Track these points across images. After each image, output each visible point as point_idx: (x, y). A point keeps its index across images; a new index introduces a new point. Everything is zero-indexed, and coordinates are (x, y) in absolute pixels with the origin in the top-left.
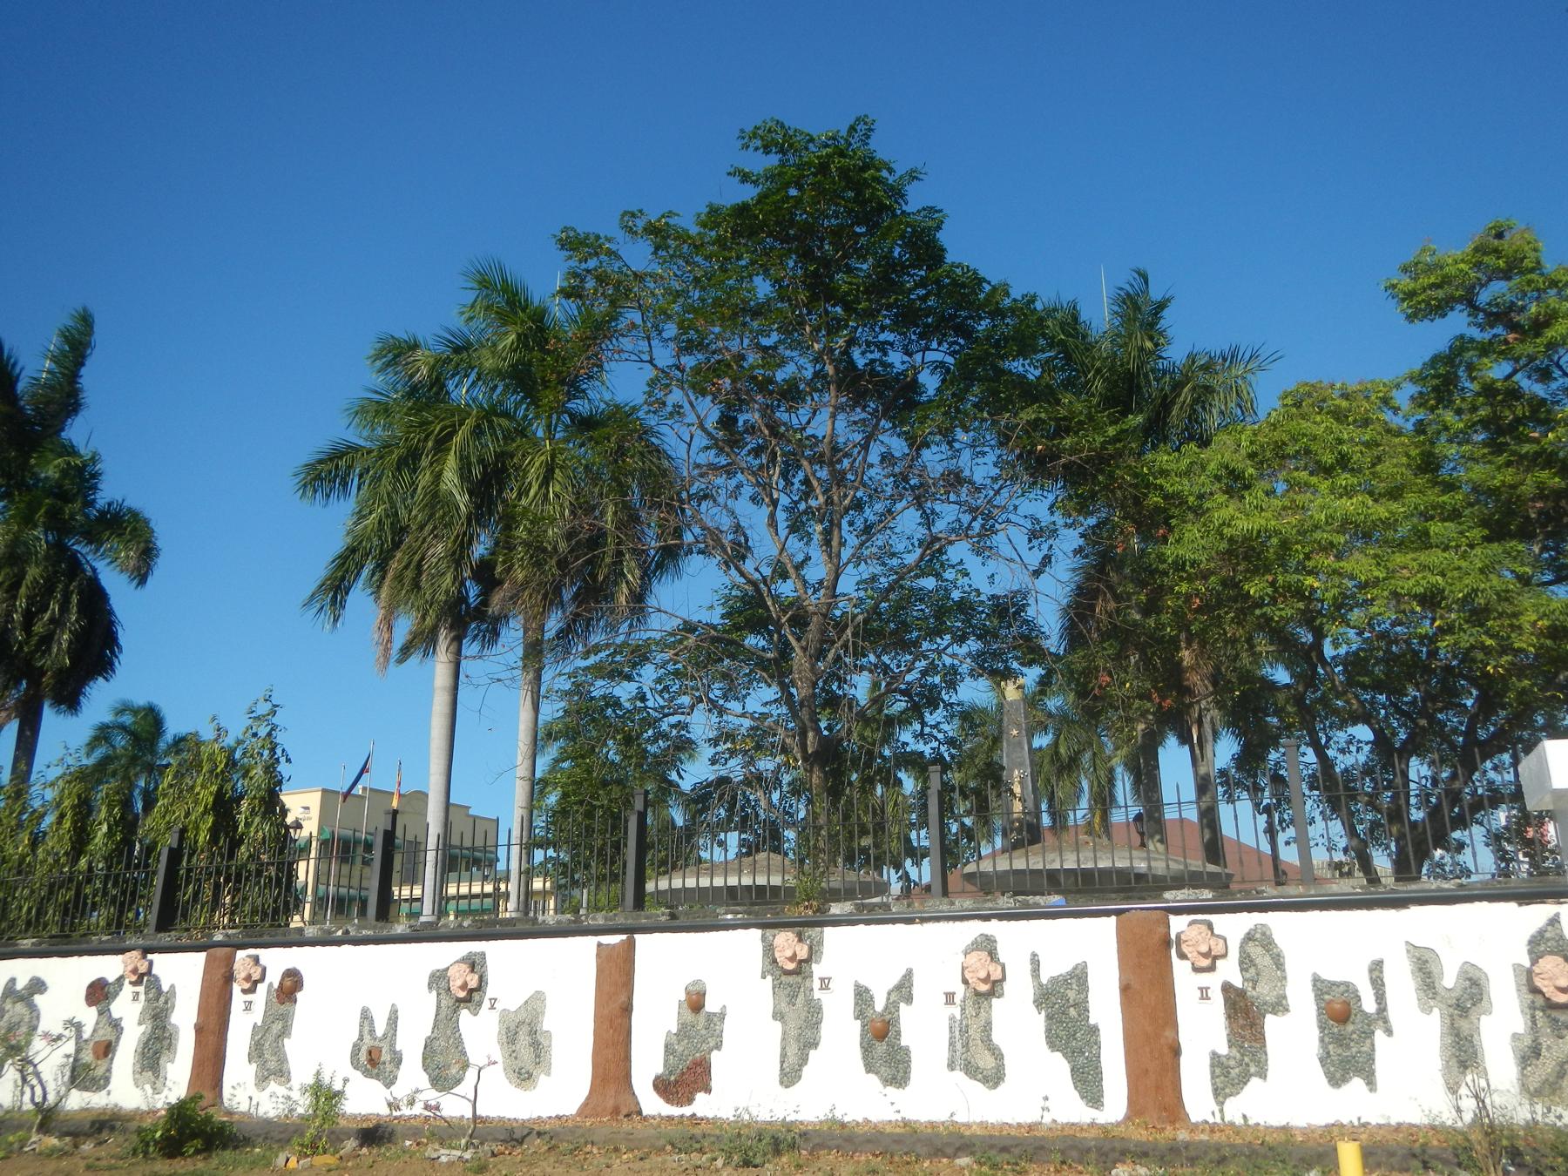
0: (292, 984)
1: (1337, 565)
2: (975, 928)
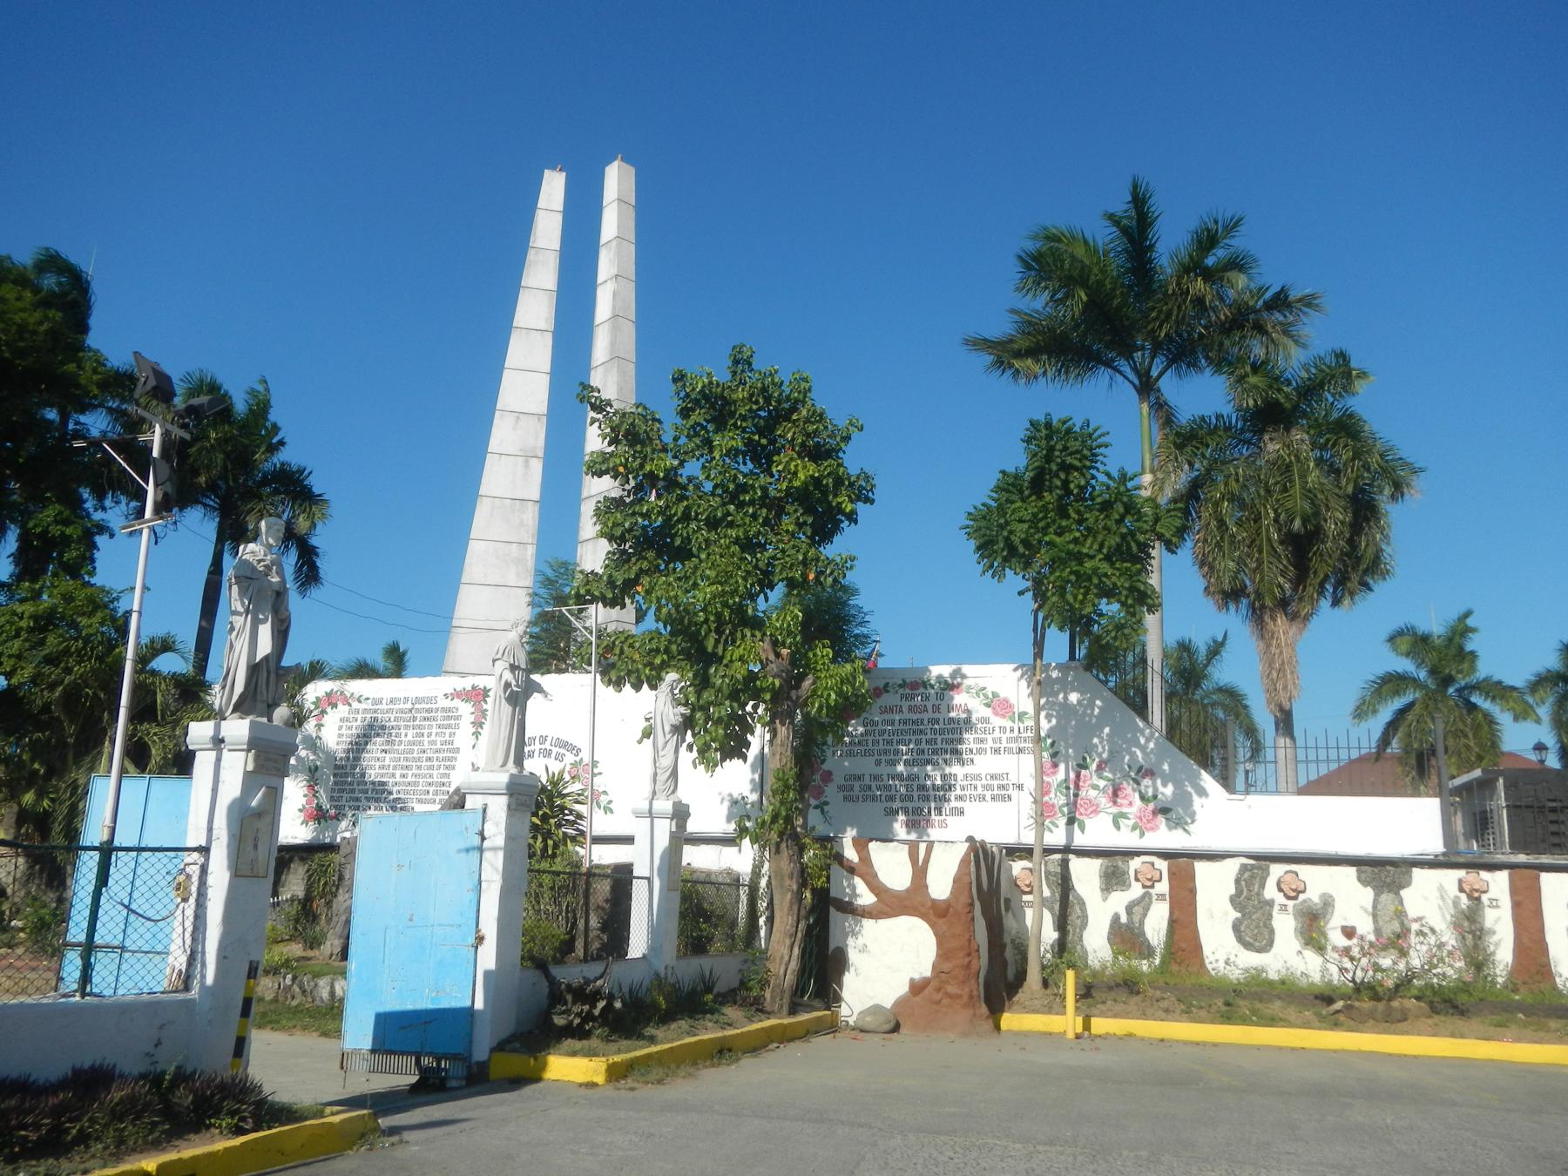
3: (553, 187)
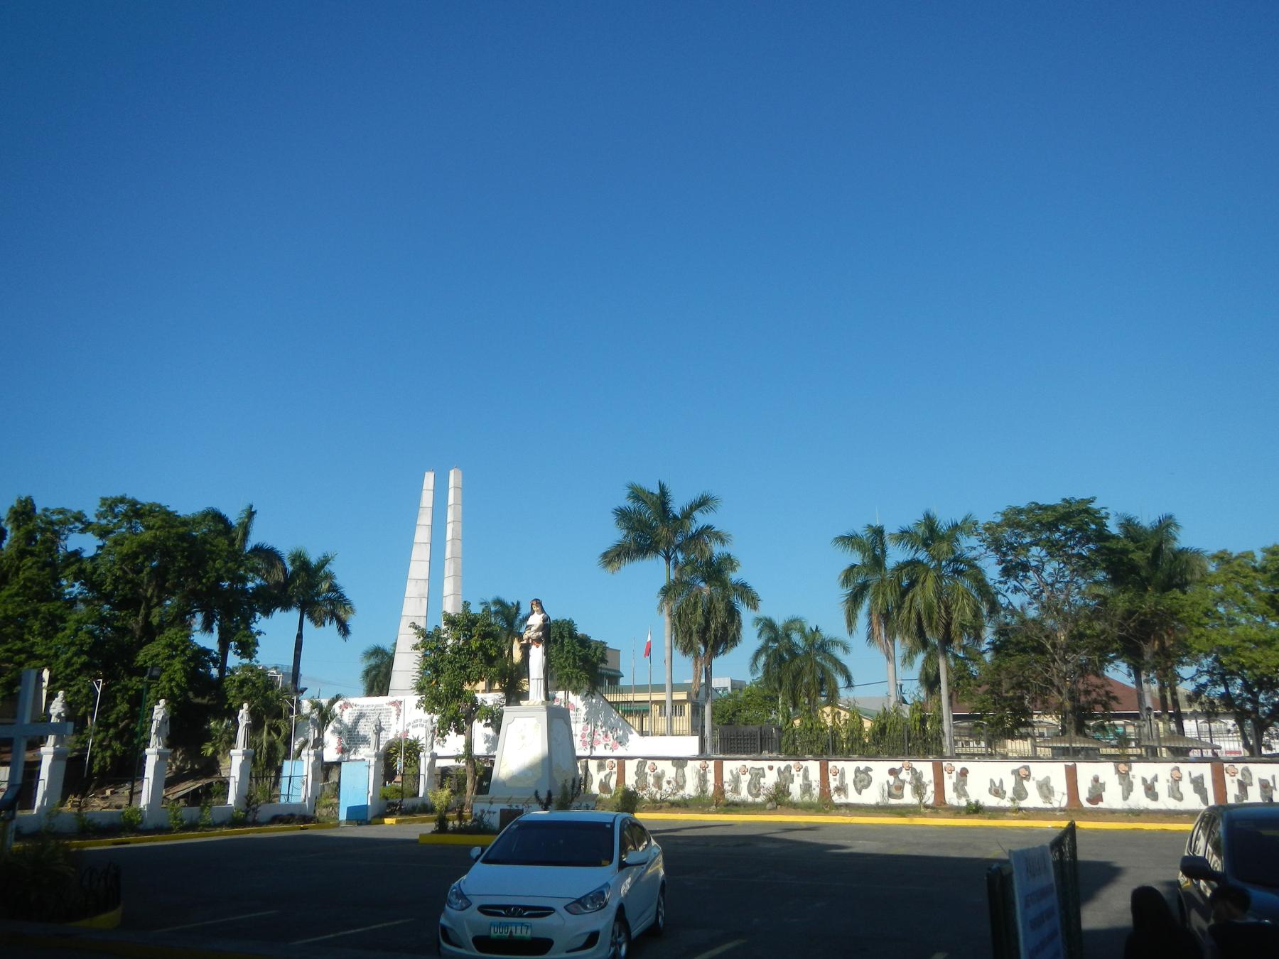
0: (964, 773)
1: (1251, 655)
2: (1173, 765)
3: (429, 479)
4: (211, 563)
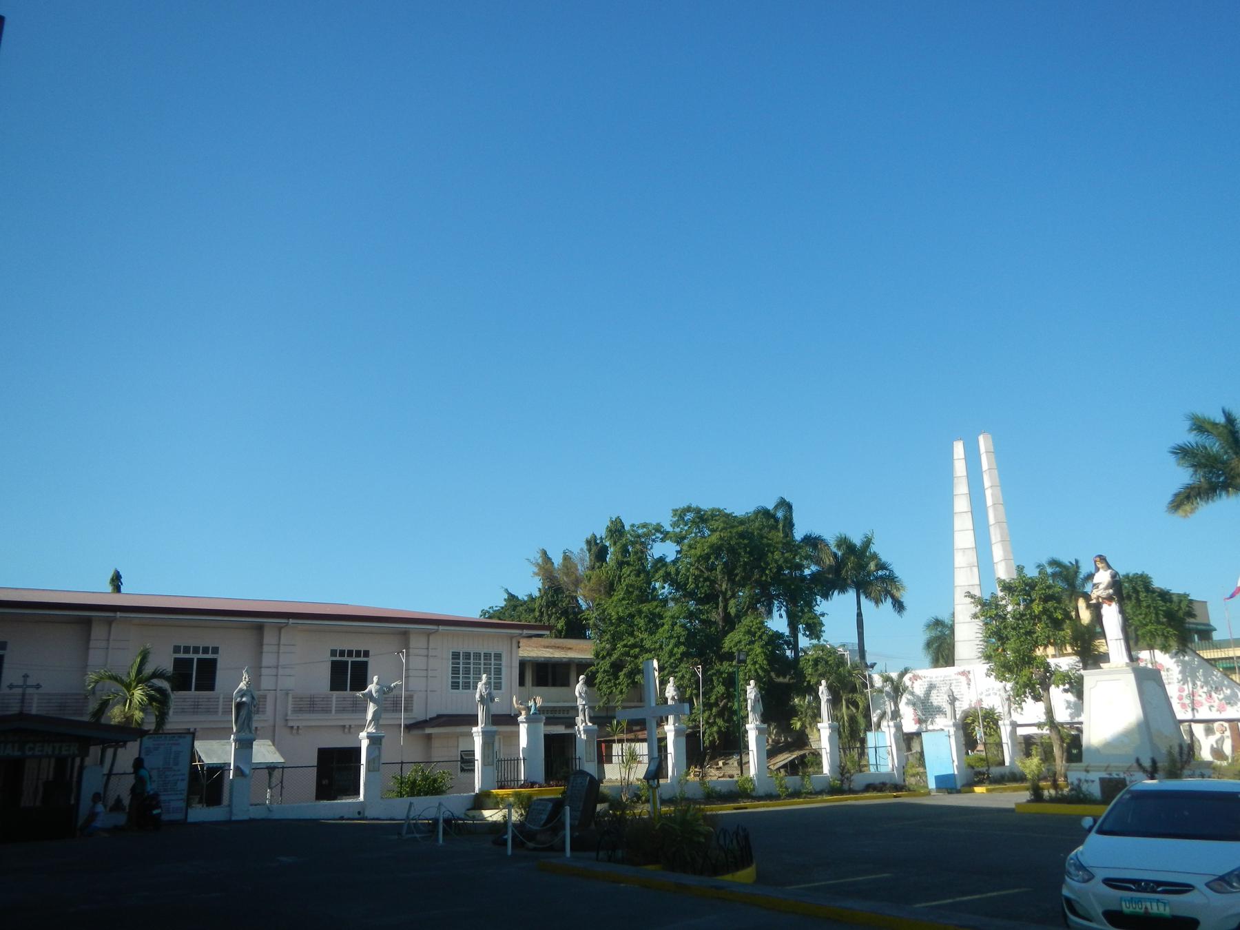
3: (959, 449)
4: (770, 554)
